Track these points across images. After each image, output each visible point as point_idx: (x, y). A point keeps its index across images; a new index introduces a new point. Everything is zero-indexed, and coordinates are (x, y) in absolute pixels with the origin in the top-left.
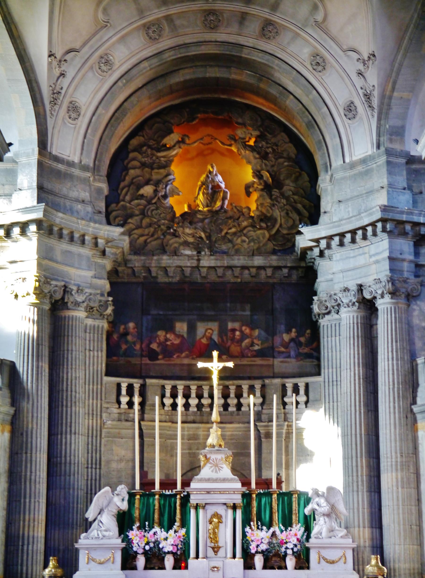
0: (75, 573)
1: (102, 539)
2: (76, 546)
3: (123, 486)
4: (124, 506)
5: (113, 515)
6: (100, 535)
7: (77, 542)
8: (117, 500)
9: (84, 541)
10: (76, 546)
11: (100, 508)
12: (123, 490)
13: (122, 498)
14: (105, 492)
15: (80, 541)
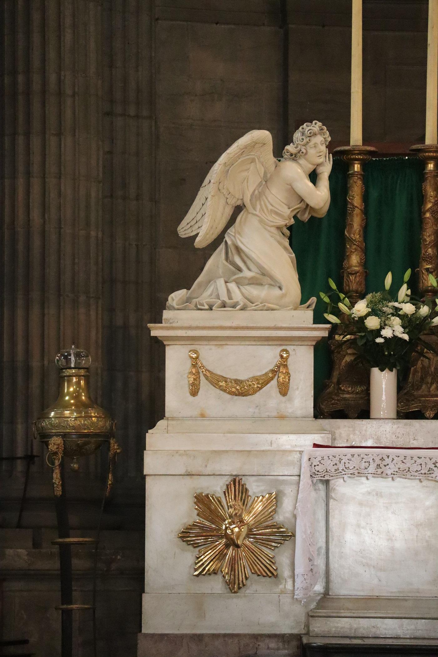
0: (152, 426)
1: (243, 309)
2: (156, 331)
3: (316, 126)
4: (320, 196)
5: (279, 228)
6: (237, 295)
7: (158, 319)
8: (294, 172)
9: (178, 317)
10: (153, 333)
11: (234, 202)
12: (313, 141)
13: (311, 168)
14: (253, 145)
15: (166, 314)
